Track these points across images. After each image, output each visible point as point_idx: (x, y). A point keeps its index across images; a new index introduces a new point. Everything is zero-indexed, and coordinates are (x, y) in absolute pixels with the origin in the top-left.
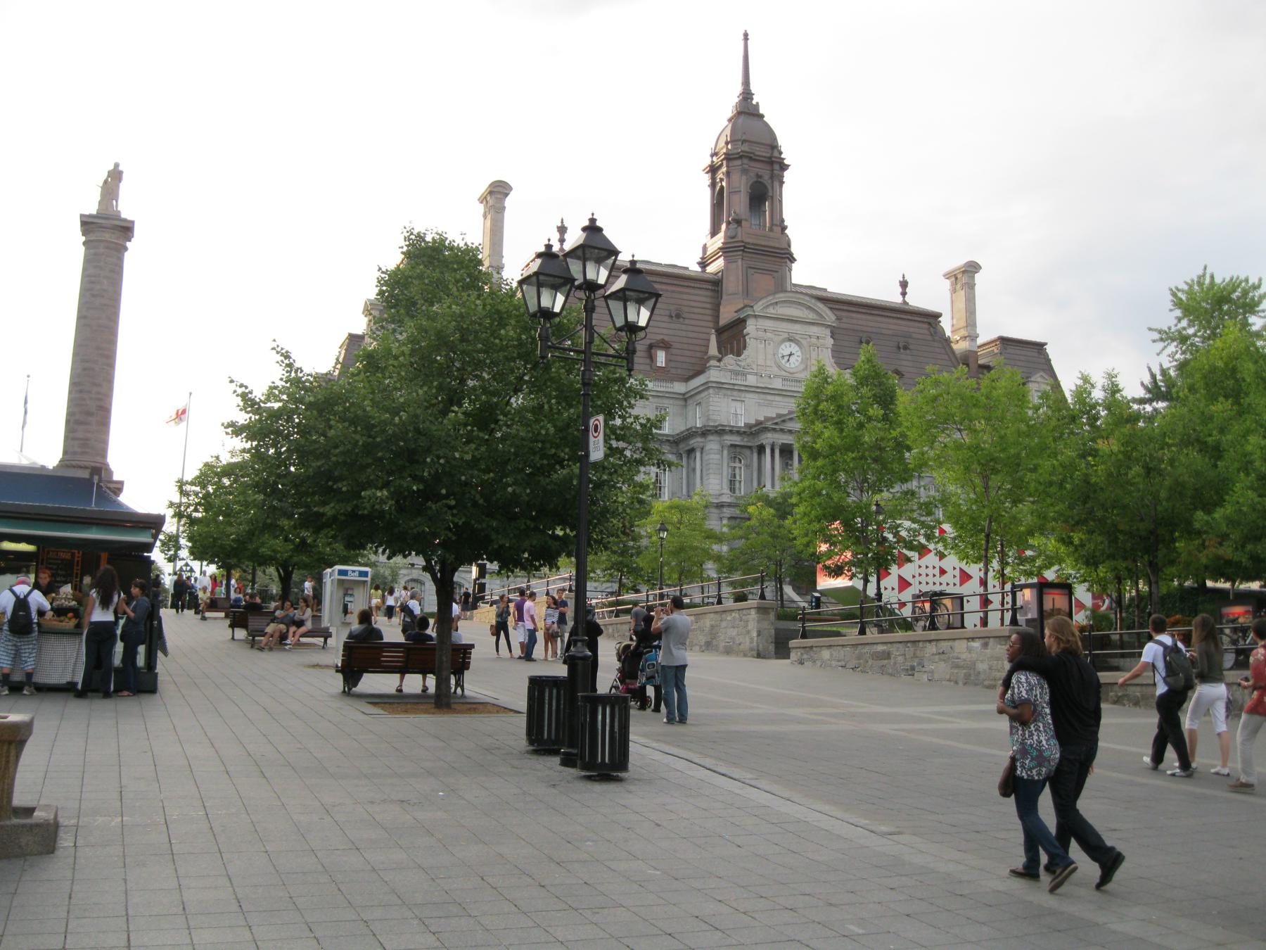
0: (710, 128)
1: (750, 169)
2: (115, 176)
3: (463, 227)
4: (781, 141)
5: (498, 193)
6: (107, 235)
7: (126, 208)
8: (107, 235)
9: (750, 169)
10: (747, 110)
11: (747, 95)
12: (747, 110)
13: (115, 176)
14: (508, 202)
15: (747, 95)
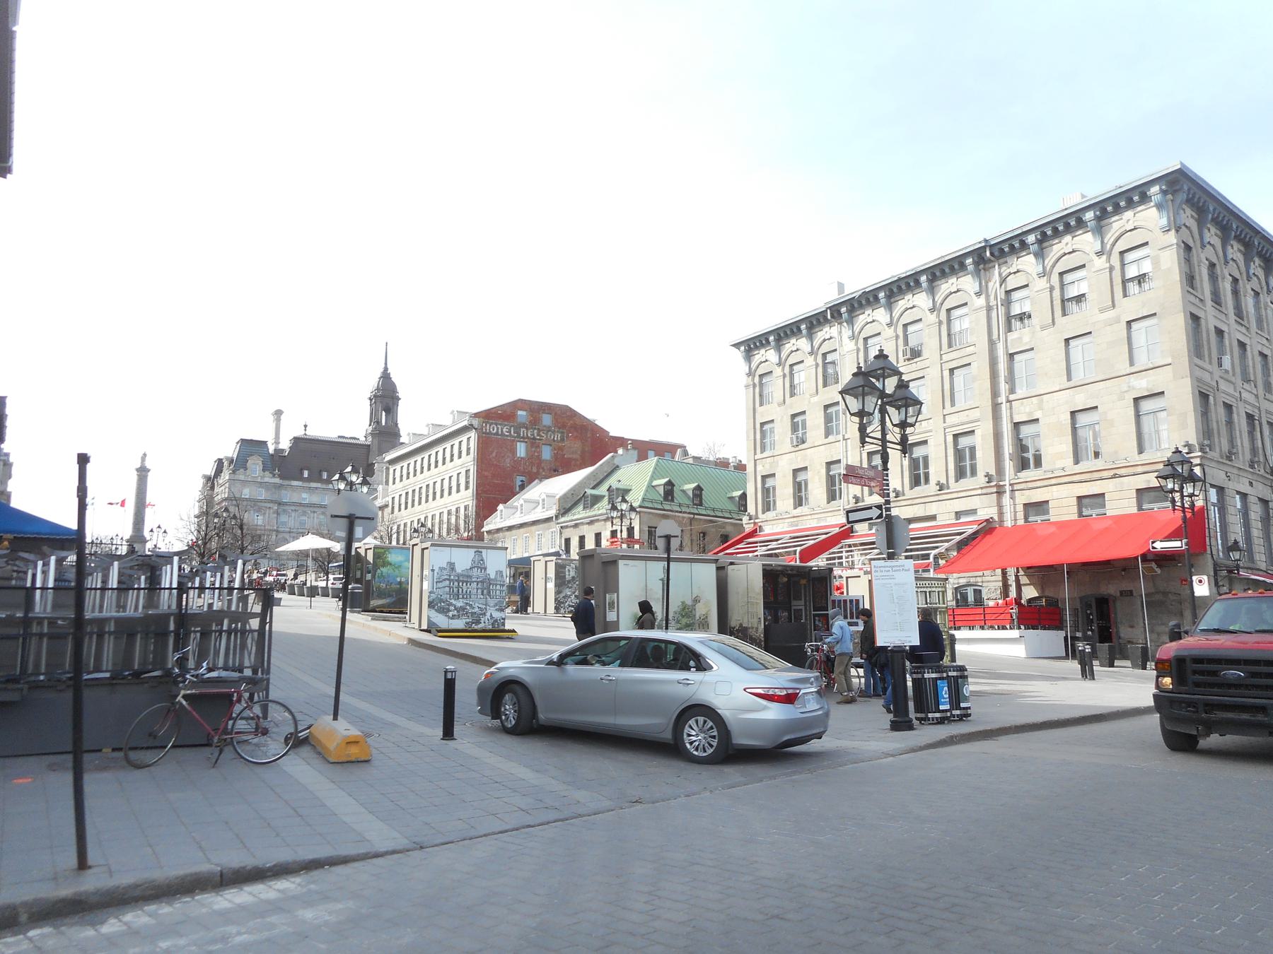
0: (371, 382)
1: (386, 398)
2: (145, 455)
3: (263, 432)
4: (399, 389)
5: (278, 413)
6: (143, 472)
7: (148, 465)
8: (143, 472)
9: (386, 398)
10: (386, 376)
11: (386, 369)
12: (386, 376)
13: (145, 455)
14: (283, 417)
15: (386, 369)
